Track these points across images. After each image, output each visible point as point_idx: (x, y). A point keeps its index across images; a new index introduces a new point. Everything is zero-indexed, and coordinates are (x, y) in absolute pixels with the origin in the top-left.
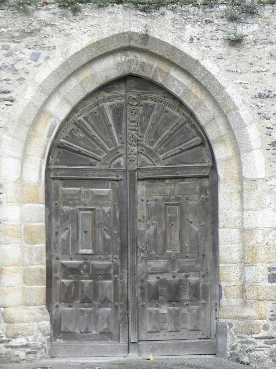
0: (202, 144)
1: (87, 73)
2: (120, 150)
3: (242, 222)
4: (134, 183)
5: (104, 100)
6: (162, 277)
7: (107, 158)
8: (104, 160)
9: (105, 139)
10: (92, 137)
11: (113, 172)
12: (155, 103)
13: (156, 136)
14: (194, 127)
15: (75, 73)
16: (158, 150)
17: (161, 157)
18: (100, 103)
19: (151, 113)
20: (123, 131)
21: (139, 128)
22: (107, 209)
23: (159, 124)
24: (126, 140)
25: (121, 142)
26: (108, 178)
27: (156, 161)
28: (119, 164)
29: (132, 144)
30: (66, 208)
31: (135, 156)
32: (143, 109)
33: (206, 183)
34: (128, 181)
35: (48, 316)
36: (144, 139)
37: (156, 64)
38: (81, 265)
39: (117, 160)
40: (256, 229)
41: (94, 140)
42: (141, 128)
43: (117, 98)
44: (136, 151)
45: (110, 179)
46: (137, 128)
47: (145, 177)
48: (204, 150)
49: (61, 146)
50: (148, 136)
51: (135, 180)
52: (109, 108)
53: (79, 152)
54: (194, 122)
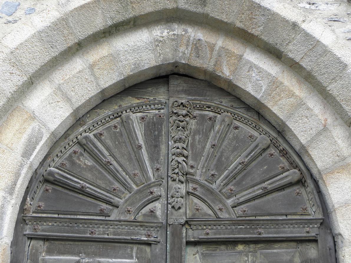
0: (301, 182)
2: (155, 189)
4: (180, 249)
7: (131, 202)
8: (125, 205)
9: (129, 169)
10: (106, 166)
11: (142, 229)
12: (216, 114)
13: (220, 166)
14: (284, 153)
16: (224, 191)
17: (230, 202)
18: (124, 112)
19: (210, 131)
20: (162, 158)
21: (190, 152)
23: (223, 147)
24: (166, 174)
25: (158, 176)
26: (132, 239)
27: (220, 210)
29: (177, 180)
31: (182, 200)
32: (197, 123)
34: (168, 246)
36: (199, 172)
39: (150, 206)
41: (110, 172)
42: (192, 153)
43: (152, 106)
44: (184, 192)
45: (136, 240)
46: (185, 152)
47: (201, 237)
48: (306, 194)
50: (206, 165)
51: (182, 243)
52: (139, 121)
53: (82, 191)
54: (285, 146)
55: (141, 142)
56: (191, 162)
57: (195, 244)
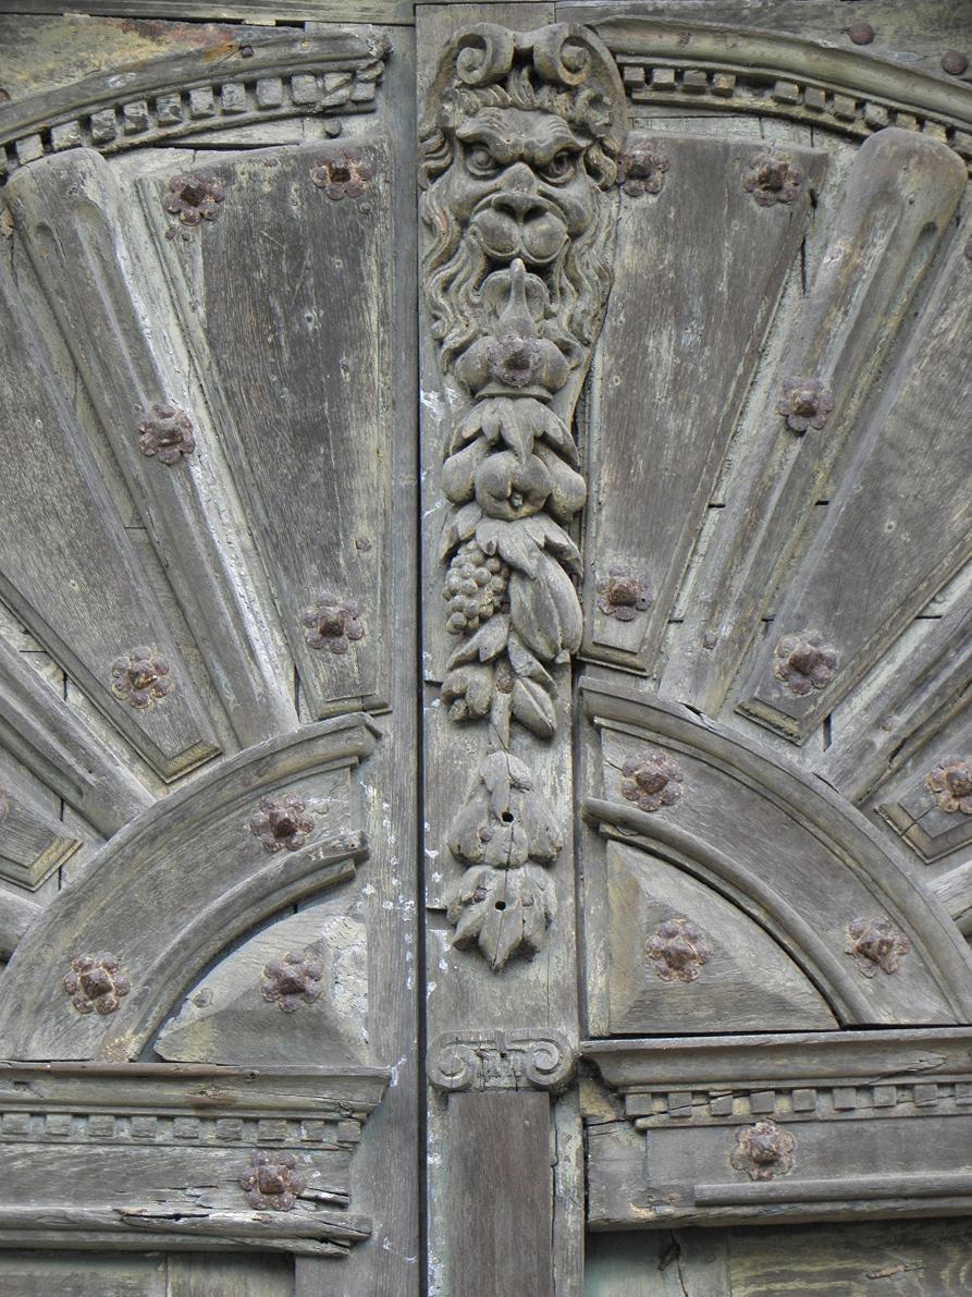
2: (313, 801)
8: (65, 939)
9: (90, 636)
11: (209, 1133)
12: (824, 145)
16: (896, 794)
18: (31, 148)
19: (772, 287)
20: (363, 529)
21: (605, 477)
23: (885, 422)
24: (403, 669)
25: (338, 688)
26: (131, 1224)
27: (871, 954)
29: (500, 716)
31: (549, 888)
32: (658, 223)
34: (437, 1268)
36: (680, 643)
39: (274, 946)
42: (624, 483)
43: (272, 91)
44: (558, 815)
45: (165, 1225)
46: (562, 479)
47: (708, 1188)
50: (738, 584)
51: (548, 1240)
52: (163, 223)
55: (183, 393)
56: (611, 562)
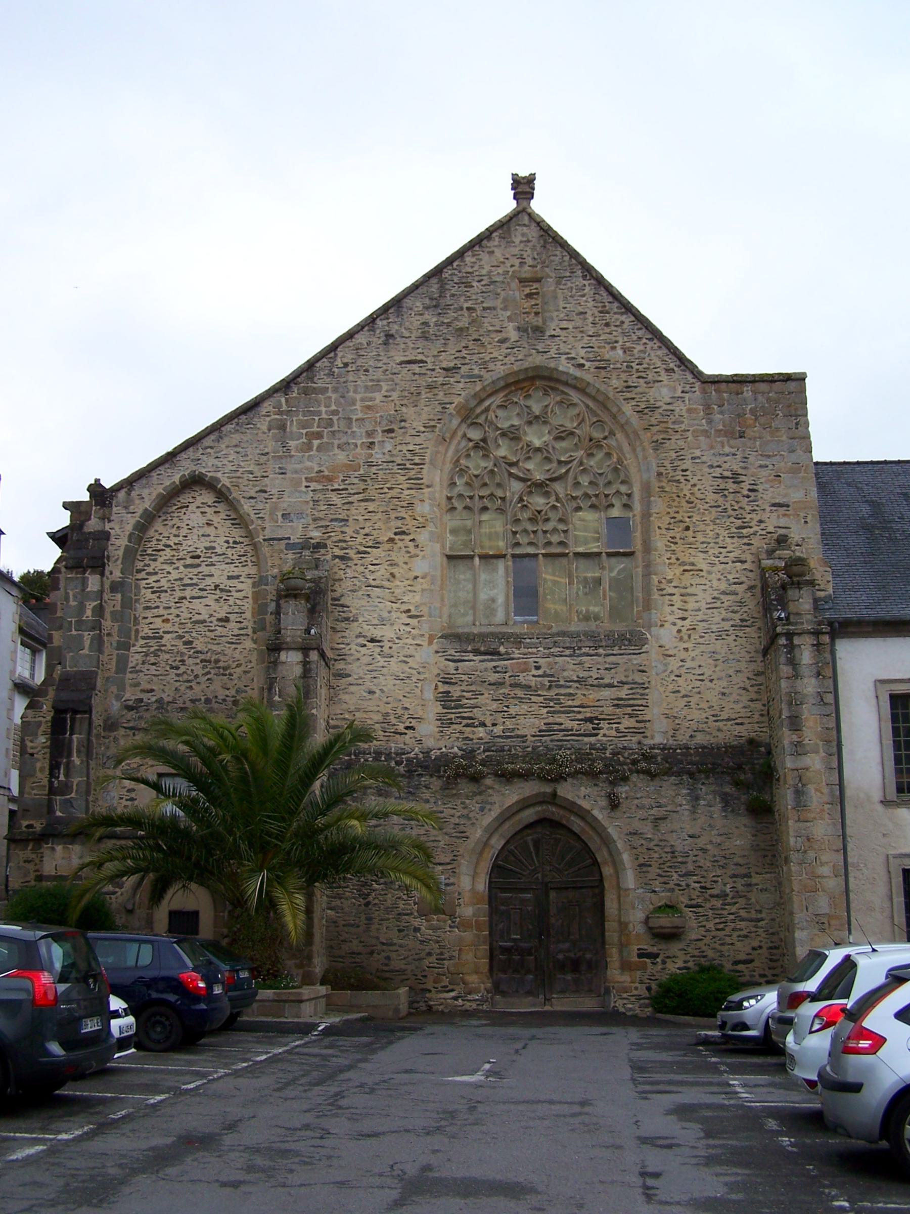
0: (593, 864)
1: (517, 818)
3: (620, 917)
5: (528, 835)
6: (567, 954)
10: (520, 860)
15: (509, 818)
17: (566, 873)
22: (529, 908)
28: (537, 878)
30: (503, 908)
33: (597, 891)
35: (490, 981)
37: (562, 812)
38: (512, 947)
40: (630, 922)
49: (499, 867)
53: (511, 870)
57: (554, 889)
